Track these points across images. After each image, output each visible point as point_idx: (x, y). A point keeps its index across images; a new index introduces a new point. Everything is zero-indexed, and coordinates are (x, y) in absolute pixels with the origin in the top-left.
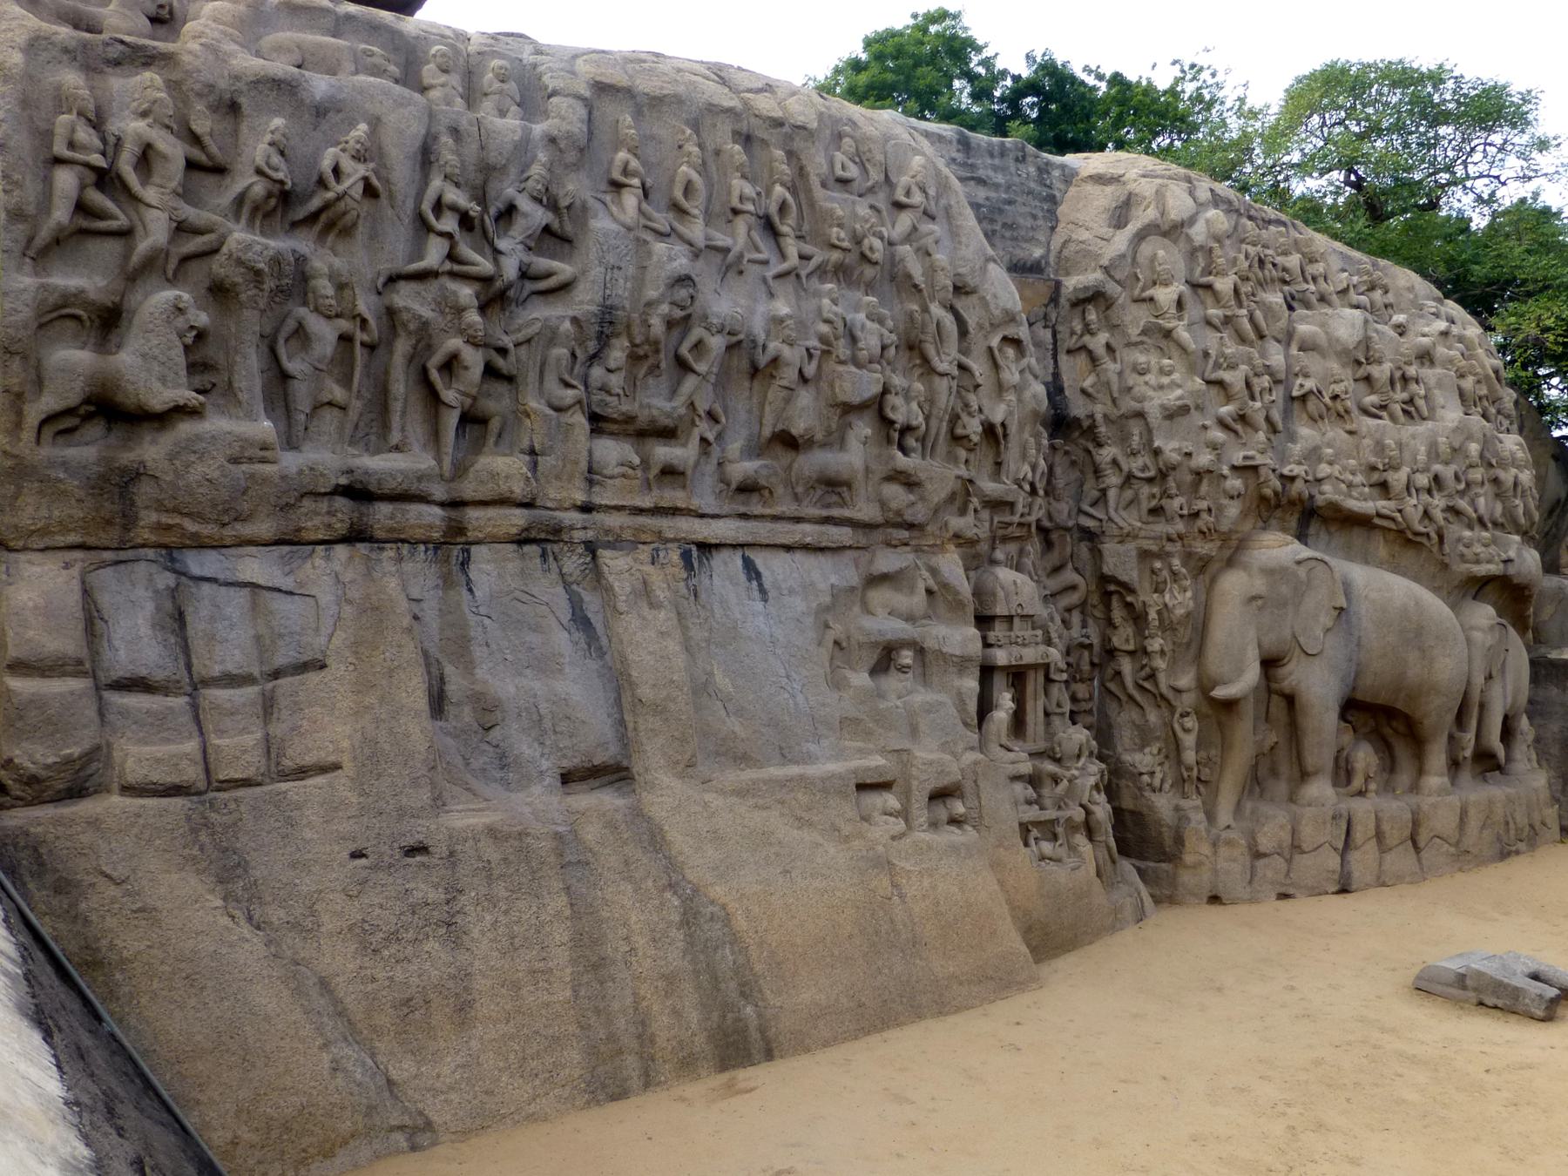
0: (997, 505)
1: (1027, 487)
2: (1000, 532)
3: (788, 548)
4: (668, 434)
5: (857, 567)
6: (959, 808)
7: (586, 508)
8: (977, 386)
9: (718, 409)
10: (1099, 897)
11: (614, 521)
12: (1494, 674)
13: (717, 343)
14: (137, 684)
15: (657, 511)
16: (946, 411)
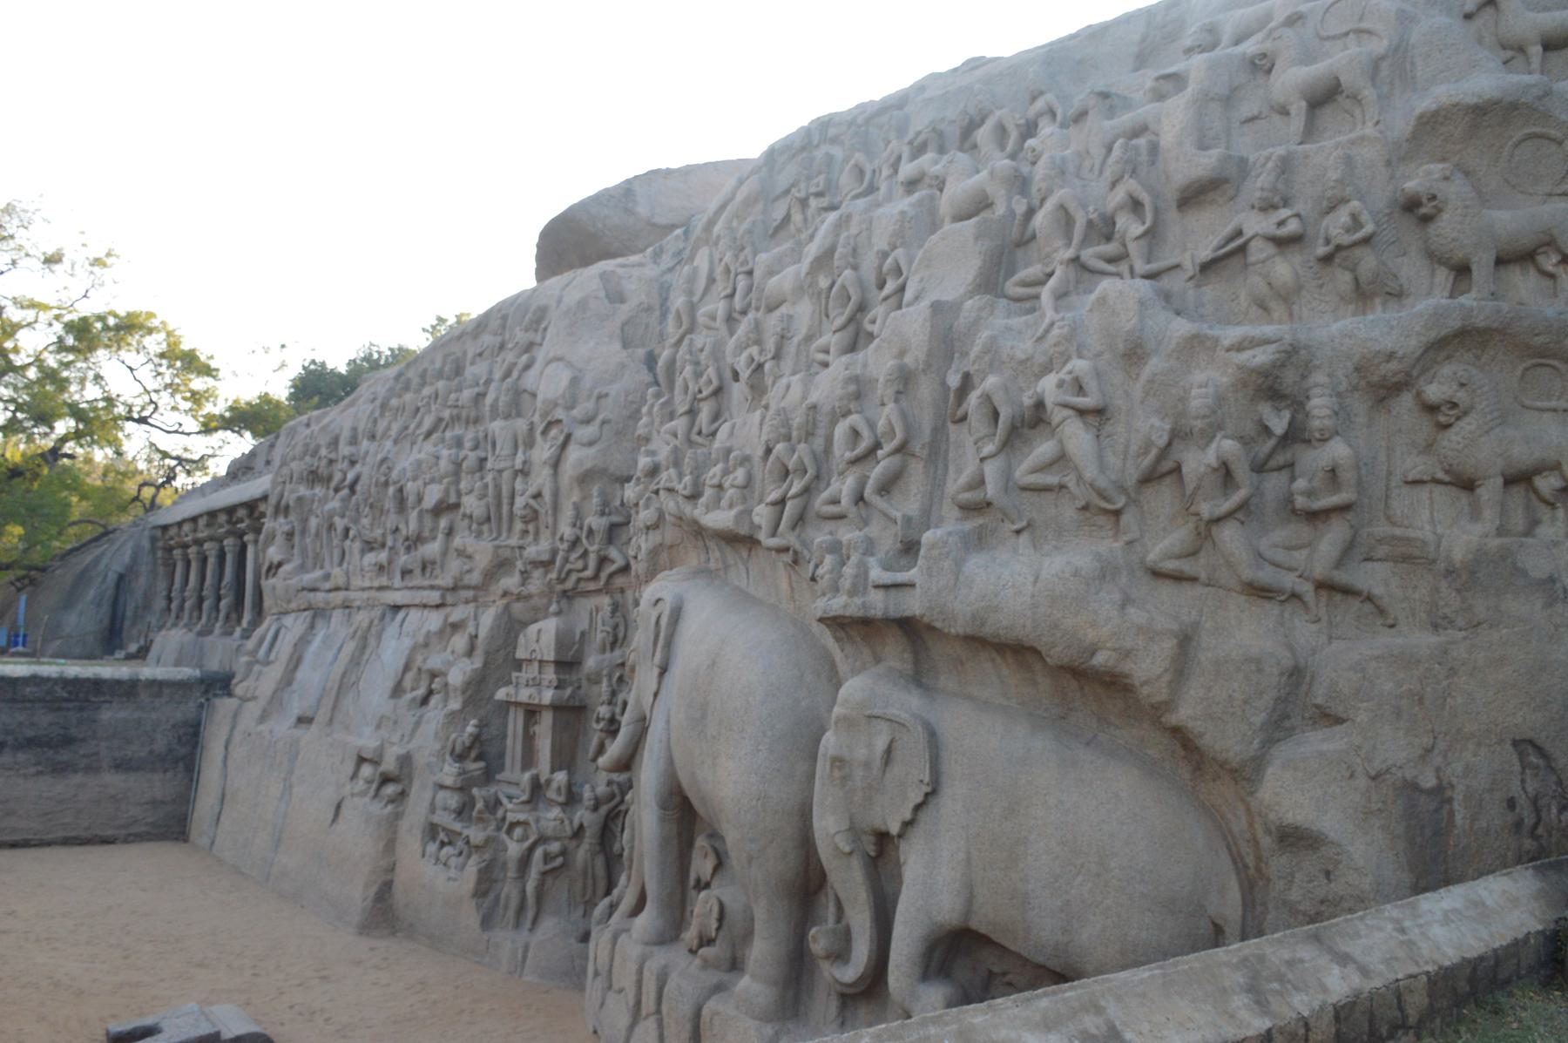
0: (547, 565)
1: (565, 546)
2: (559, 588)
3: (425, 606)
4: (383, 545)
5: (446, 617)
6: (390, 789)
7: (363, 589)
8: (521, 471)
9: (402, 526)
10: (470, 917)
11: (365, 595)
12: (894, 829)
13: (391, 490)
14: (257, 662)
15: (381, 588)
16: (498, 496)
